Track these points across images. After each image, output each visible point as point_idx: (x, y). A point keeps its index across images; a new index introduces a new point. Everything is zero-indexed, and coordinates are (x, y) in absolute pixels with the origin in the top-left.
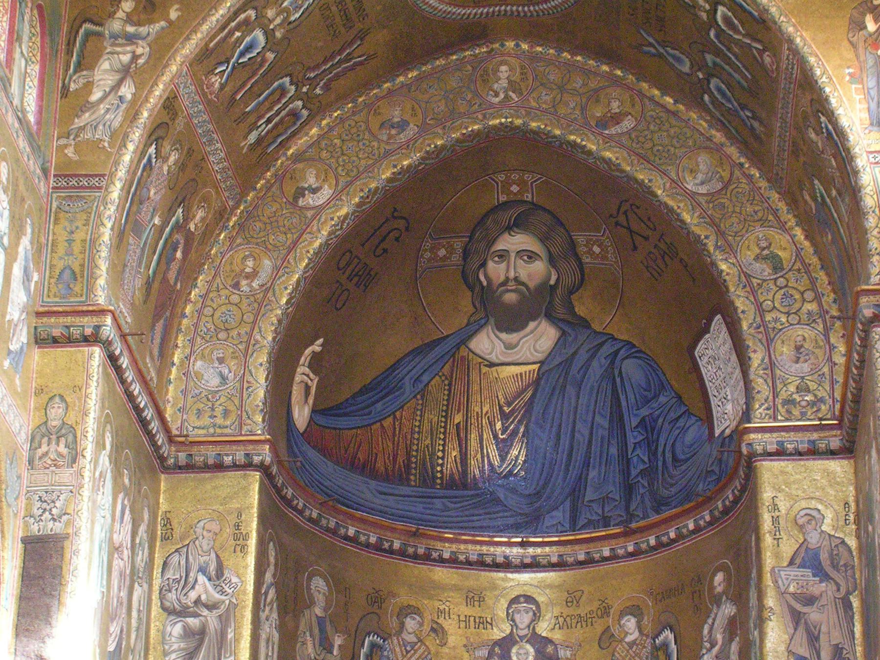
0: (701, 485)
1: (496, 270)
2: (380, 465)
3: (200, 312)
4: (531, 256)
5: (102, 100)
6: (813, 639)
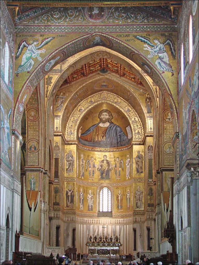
0: (126, 144)
1: (102, 117)
2: (88, 140)
3: (68, 125)
4: (107, 115)
5: (59, 106)
6: (138, 166)
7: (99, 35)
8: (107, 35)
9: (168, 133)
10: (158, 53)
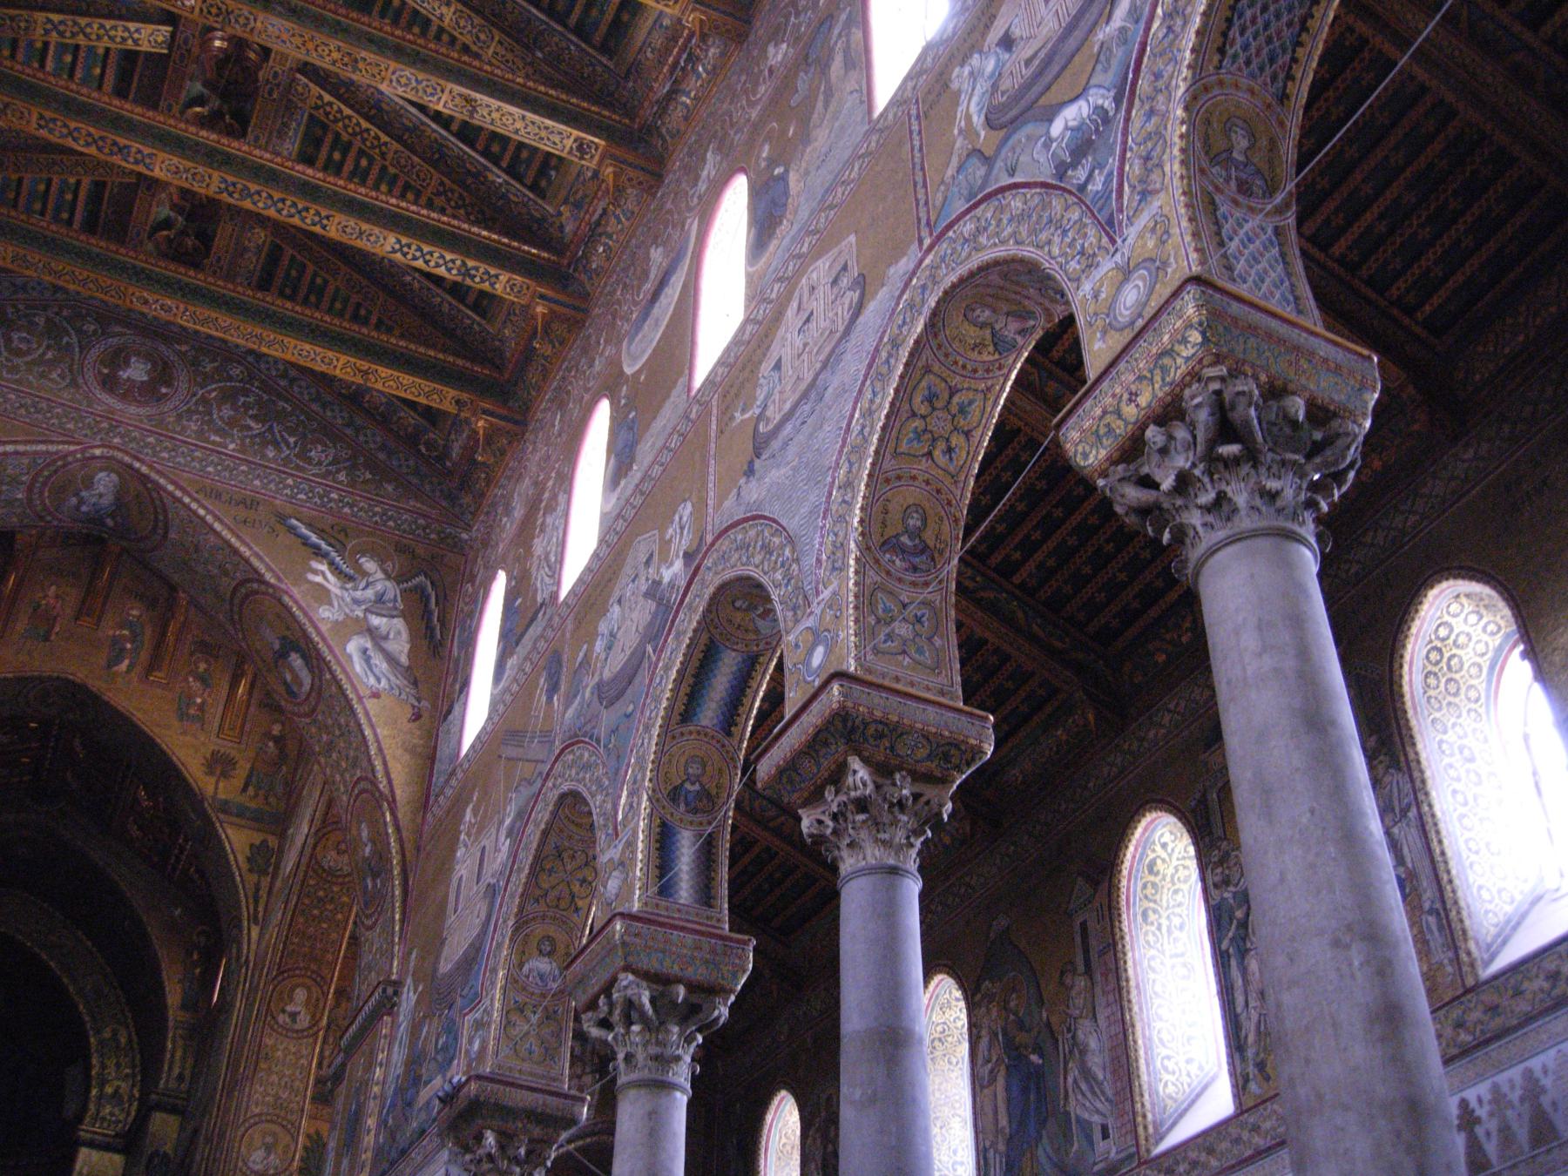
7: (120, 462)
8: (158, 472)
9: (274, 1078)
10: (366, 610)
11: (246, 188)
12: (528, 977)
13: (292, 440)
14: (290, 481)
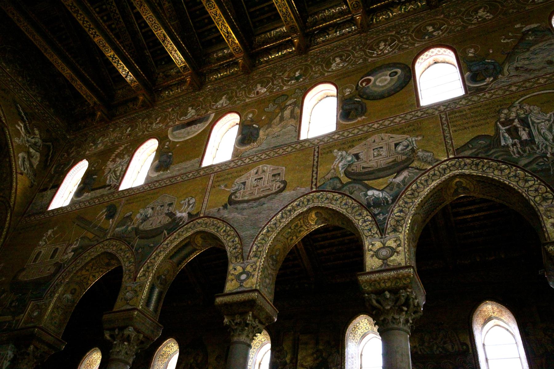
10: (30, 145)
11: (78, 10)
12: (64, 299)
13: (28, 79)
14: (22, 92)
